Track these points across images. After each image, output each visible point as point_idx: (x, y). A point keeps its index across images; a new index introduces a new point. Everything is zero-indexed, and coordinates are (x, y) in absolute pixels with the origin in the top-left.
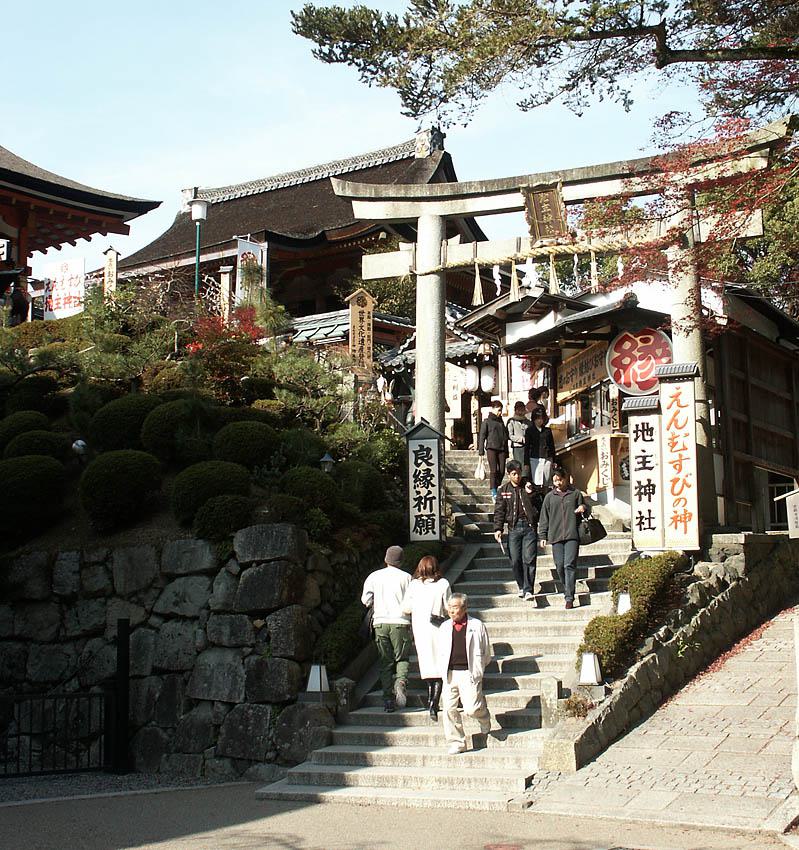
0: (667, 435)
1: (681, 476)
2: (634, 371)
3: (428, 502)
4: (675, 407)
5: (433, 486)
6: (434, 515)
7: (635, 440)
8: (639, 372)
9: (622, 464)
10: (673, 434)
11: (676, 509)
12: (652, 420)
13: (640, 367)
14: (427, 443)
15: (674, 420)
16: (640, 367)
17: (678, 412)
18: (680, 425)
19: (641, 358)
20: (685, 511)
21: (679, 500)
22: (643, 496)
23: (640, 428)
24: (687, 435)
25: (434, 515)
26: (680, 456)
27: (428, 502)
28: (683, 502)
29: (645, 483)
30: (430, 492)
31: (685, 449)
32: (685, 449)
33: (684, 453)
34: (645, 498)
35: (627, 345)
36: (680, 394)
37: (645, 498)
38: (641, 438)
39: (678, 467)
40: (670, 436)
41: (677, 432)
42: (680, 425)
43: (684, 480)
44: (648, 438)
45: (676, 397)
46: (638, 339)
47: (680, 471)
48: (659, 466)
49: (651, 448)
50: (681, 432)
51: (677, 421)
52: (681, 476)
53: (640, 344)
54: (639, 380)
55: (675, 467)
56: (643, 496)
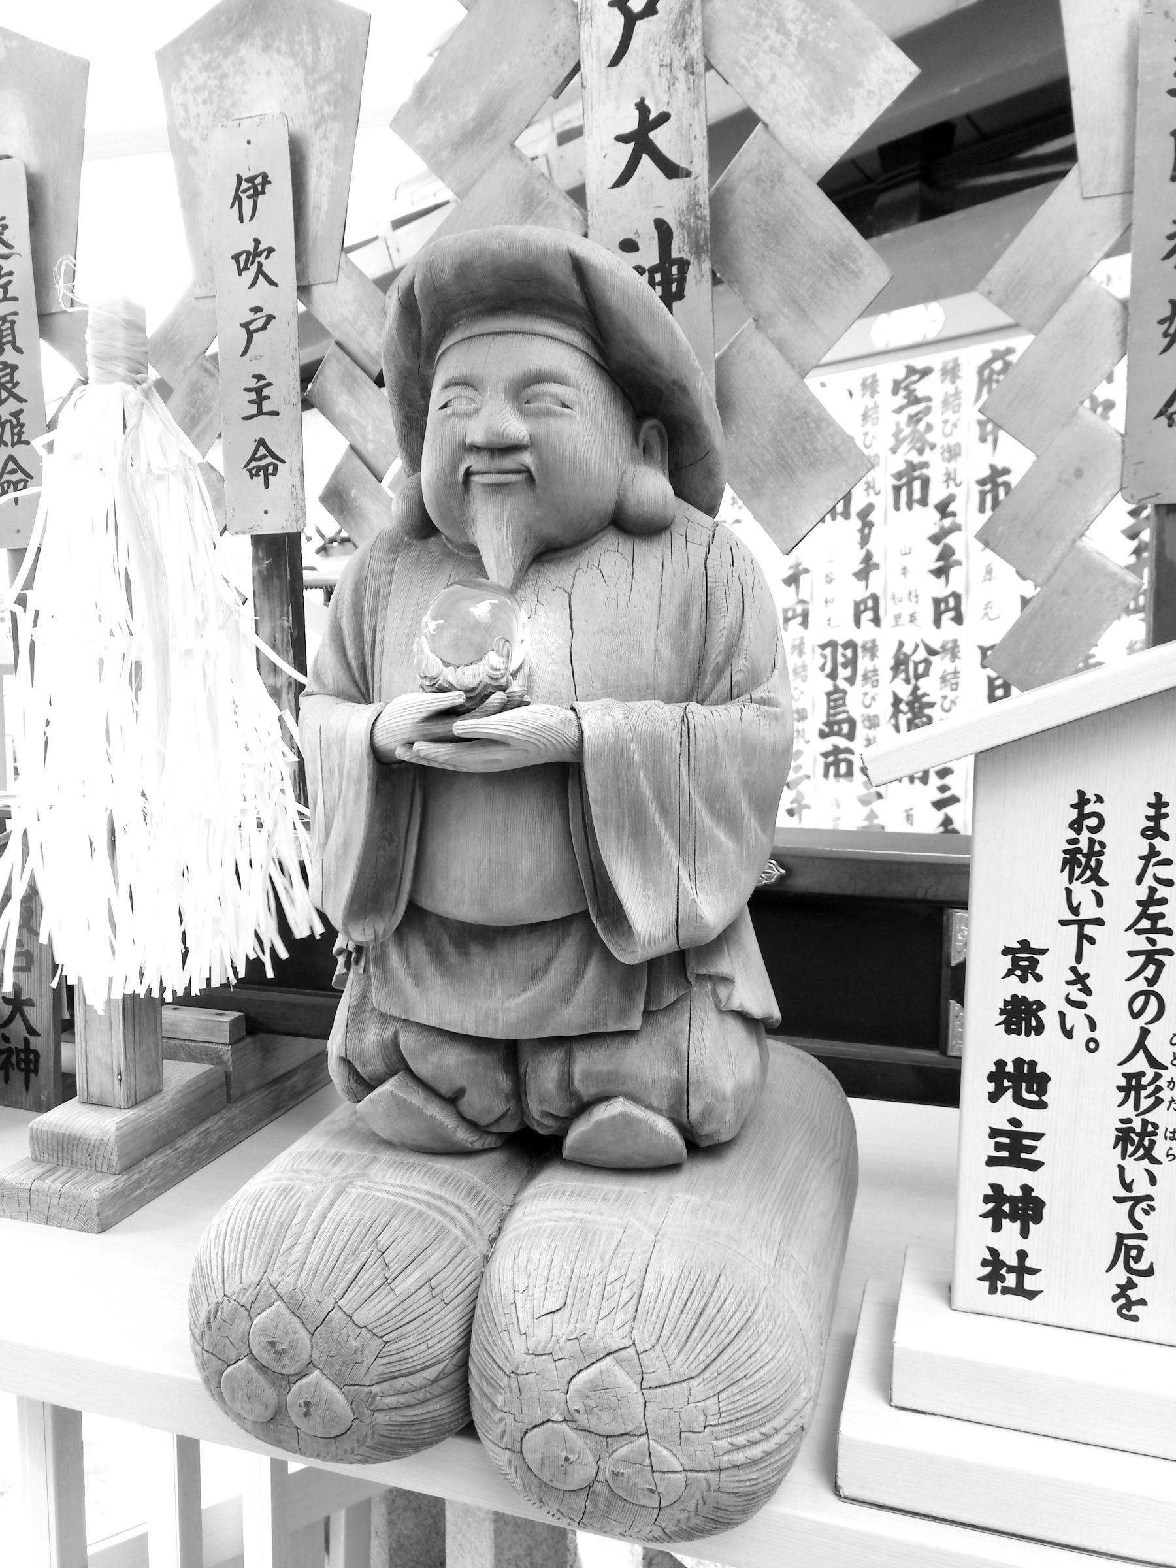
22: (1006, 1222)
23: (1010, 1068)
29: (1012, 1189)
34: (1011, 1228)
38: (1010, 1093)
44: (1033, 1097)
56: (1006, 1222)
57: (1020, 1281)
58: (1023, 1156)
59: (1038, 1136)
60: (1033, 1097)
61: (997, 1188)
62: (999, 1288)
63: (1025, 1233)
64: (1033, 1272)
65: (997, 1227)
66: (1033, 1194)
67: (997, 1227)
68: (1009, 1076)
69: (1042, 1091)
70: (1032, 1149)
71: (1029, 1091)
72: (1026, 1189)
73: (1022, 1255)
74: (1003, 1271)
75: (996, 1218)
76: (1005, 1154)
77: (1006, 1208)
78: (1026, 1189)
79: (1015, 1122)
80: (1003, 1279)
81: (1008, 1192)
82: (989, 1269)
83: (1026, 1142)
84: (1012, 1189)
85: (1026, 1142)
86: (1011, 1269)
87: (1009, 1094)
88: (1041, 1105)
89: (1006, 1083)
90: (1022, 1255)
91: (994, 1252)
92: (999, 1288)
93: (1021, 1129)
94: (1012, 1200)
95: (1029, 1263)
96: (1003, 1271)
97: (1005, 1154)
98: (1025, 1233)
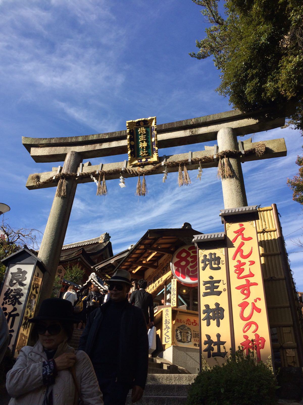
0: (233, 264)
1: (250, 300)
2: (187, 268)
3: (11, 318)
4: (239, 240)
5: (20, 303)
6: (13, 331)
7: (204, 269)
8: (191, 269)
9: (177, 330)
10: (239, 261)
11: (246, 334)
12: (220, 252)
13: (191, 267)
14: (24, 267)
15: (239, 250)
16: (191, 267)
17: (242, 244)
18: (245, 254)
19: (192, 262)
20: (257, 336)
21: (249, 325)
22: (211, 321)
24: (252, 263)
25: (13, 331)
26: (248, 281)
27: (11, 318)
28: (253, 327)
29: (212, 306)
30: (15, 309)
31: (252, 275)
32: (252, 275)
33: (252, 280)
34: (213, 323)
35: (184, 255)
36: (244, 229)
37: (213, 323)
38: (208, 267)
39: (245, 292)
40: (237, 264)
41: (243, 261)
42: (245, 254)
43: (253, 304)
45: (240, 232)
46: (191, 252)
47: (248, 295)
48: (227, 291)
49: (220, 275)
50: (246, 261)
51: (242, 251)
52: (250, 300)
53: (192, 254)
54: (191, 274)
55: (243, 293)
56: (211, 321)
57: (219, 349)
58: (215, 290)
59: (219, 282)
60: (216, 266)
61: (207, 306)
62: (212, 354)
63: (218, 325)
64: (223, 343)
65: (208, 324)
66: (220, 306)
67: (208, 324)
68: (208, 260)
69: (219, 263)
70: (218, 287)
71: (215, 264)
72: (217, 305)
73: (219, 336)
74: (212, 346)
75: (208, 319)
76: (209, 291)
77: (211, 314)
78: (217, 305)
79: (211, 277)
80: (213, 349)
81: (211, 307)
82: (207, 345)
83: (215, 284)
84: (212, 306)
85: (215, 284)
86: (215, 344)
87: (208, 267)
88: (219, 268)
89: (207, 263)
90: (219, 336)
91: (208, 337)
92: (212, 354)
93: (214, 280)
94: (213, 310)
95: (222, 339)
96: (212, 346)
97: (209, 291)
98: (218, 325)
